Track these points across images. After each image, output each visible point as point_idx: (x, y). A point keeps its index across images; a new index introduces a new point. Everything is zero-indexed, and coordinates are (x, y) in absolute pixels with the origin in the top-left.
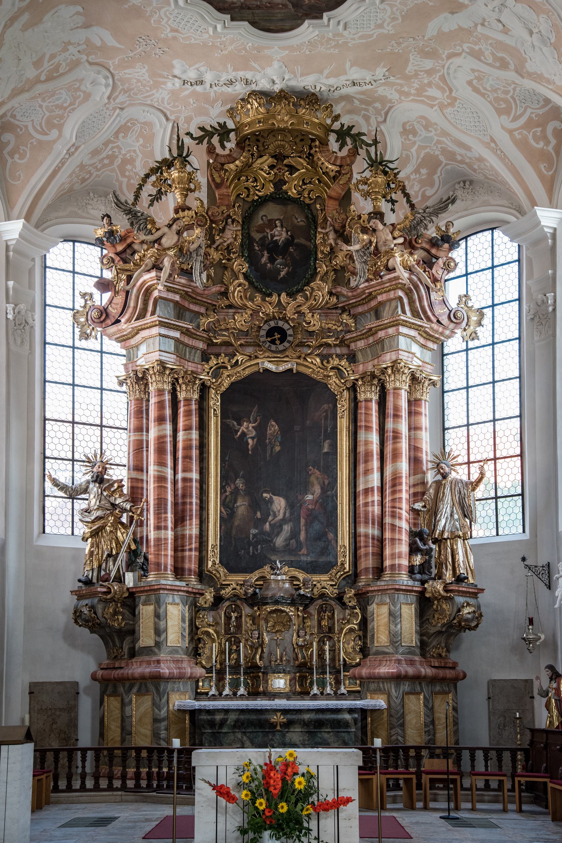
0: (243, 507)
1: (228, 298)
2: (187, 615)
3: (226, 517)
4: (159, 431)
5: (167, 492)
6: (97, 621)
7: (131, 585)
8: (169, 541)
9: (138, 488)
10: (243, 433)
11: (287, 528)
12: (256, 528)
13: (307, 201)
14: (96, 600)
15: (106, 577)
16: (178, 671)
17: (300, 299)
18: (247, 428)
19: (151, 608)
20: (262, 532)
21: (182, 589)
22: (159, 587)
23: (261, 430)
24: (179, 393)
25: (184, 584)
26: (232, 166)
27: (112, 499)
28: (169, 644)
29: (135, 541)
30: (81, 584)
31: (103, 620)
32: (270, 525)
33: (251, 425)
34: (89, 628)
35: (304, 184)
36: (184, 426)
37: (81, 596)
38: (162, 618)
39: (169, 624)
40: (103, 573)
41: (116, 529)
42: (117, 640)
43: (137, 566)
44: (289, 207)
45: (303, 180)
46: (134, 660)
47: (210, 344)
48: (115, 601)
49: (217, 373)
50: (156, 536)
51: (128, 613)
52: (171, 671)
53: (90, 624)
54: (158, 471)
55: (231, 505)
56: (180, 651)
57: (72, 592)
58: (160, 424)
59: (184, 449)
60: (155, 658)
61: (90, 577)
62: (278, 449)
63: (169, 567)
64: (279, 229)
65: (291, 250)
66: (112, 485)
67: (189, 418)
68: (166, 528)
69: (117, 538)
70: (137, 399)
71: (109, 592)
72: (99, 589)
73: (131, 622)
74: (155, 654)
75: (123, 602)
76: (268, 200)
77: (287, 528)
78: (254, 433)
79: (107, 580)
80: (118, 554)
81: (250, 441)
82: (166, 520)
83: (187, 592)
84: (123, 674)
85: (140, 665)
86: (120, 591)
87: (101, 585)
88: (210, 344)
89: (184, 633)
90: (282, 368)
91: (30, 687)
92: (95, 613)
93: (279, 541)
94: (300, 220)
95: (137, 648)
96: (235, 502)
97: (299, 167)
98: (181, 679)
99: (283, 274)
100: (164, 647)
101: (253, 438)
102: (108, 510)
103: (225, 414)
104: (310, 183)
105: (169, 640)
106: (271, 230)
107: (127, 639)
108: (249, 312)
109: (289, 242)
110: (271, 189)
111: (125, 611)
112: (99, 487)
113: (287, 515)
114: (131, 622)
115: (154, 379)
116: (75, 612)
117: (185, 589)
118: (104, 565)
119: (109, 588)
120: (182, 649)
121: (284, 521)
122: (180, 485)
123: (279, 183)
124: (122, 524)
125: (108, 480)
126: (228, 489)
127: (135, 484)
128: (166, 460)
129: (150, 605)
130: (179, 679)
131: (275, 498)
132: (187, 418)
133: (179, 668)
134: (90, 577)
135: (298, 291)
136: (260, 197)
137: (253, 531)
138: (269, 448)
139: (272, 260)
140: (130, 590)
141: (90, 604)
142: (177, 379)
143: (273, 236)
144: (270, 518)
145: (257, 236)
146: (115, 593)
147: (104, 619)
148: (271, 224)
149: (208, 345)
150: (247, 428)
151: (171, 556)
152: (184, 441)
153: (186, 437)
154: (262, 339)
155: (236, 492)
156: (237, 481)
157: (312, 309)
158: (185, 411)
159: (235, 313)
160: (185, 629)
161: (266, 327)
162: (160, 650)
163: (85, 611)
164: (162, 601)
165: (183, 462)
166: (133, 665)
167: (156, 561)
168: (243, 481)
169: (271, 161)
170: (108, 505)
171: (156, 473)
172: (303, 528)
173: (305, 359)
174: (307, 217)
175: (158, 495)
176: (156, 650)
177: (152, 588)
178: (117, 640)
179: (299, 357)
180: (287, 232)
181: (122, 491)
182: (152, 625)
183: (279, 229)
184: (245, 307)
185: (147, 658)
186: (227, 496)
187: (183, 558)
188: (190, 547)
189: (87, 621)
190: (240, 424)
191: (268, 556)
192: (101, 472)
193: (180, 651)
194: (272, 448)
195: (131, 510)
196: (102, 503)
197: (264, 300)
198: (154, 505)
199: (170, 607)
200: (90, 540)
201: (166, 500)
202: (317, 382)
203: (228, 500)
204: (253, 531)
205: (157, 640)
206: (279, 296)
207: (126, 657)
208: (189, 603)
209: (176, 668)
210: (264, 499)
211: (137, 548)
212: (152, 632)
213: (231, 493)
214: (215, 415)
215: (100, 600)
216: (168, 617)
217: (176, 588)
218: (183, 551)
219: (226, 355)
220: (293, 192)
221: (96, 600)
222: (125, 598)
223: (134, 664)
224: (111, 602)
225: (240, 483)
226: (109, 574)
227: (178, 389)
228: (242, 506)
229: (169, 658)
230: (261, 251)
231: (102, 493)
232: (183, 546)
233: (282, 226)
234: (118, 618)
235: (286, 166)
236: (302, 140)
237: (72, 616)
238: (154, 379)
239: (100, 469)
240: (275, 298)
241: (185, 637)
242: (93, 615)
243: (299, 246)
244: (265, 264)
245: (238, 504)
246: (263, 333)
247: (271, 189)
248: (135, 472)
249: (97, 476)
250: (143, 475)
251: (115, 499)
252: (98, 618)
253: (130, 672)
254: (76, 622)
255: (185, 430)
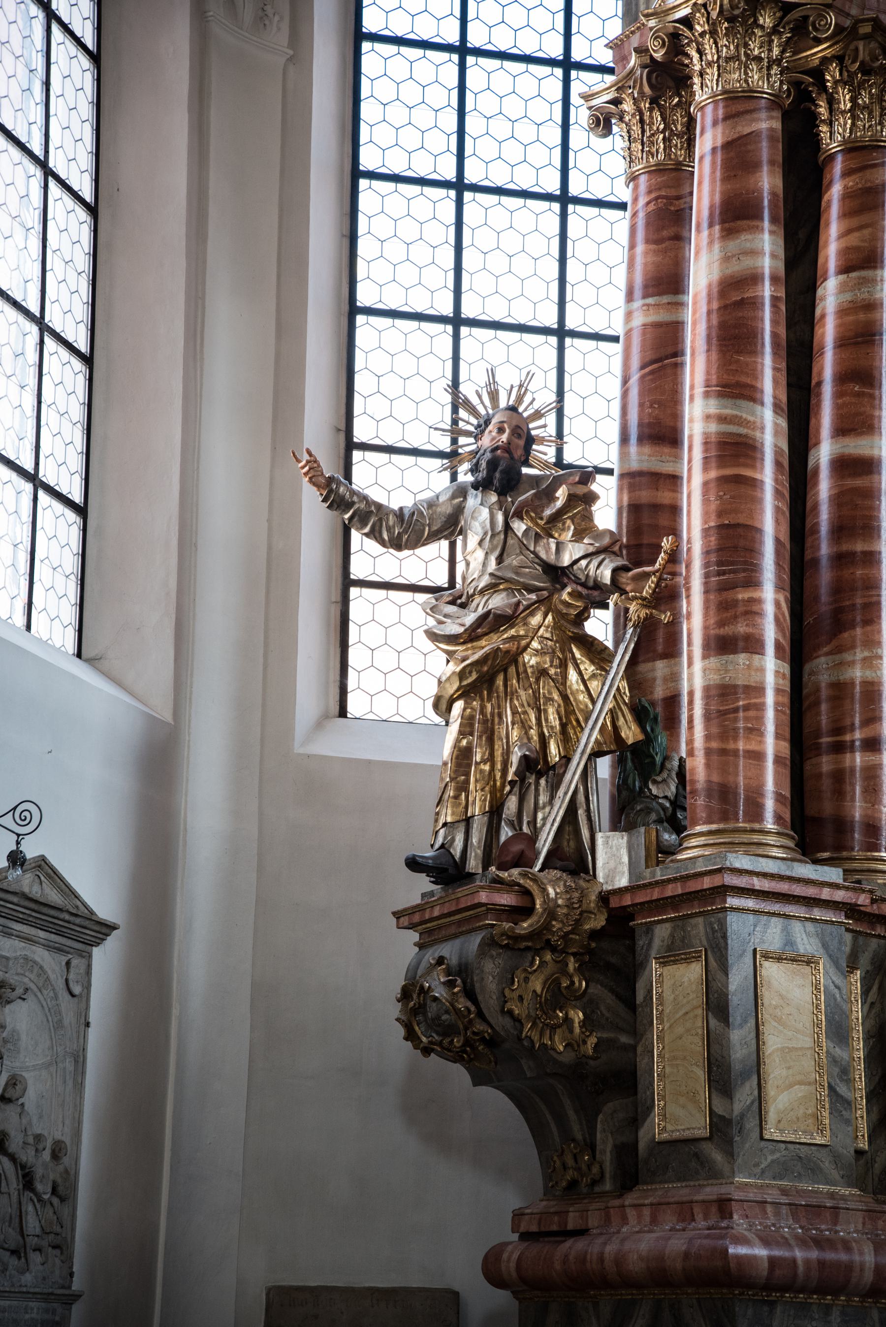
2: (857, 1012)
4: (726, 259)
5: (760, 501)
6: (479, 1026)
7: (623, 881)
8: (770, 698)
9: (656, 507)
14: (475, 941)
15: (516, 848)
16: (814, 1254)
19: (693, 972)
21: (826, 894)
22: (717, 881)
24: (824, 128)
25: (834, 874)
27: (547, 550)
28: (772, 1132)
29: (640, 714)
30: (423, 883)
31: (501, 1023)
34: (457, 1057)
36: (844, 252)
37: (430, 932)
38: (736, 1016)
39: (773, 1042)
40: (506, 833)
41: (563, 665)
42: (571, 1114)
43: (648, 811)
46: (630, 1199)
48: (554, 949)
50: (715, 678)
51: (609, 999)
52: (777, 1253)
53: (457, 1042)
54: (722, 419)
56: (827, 1165)
57: (398, 915)
58: (729, 233)
59: (842, 343)
60: (710, 1192)
61: (457, 849)
63: (770, 804)
66: (549, 495)
67: (865, 218)
68: (754, 645)
69: (565, 698)
70: (658, 170)
71: (527, 911)
72: (483, 897)
73: (624, 1039)
74: (714, 1174)
75: (590, 952)
79: (523, 860)
80: (566, 759)
82: (752, 610)
83: (851, 910)
84: (582, 1259)
85: (654, 1221)
86: (569, 906)
87: (498, 881)
89: (842, 1089)
91: (268, 1294)
92: (470, 994)
95: (642, 1145)
98: (836, 1293)
100: (747, 1145)
102: (530, 589)
105: (772, 1116)
107: (609, 1107)
111: (596, 990)
112: (500, 504)
114: (624, 1039)
115: (710, 54)
116: (406, 994)
117: (840, 896)
118: (512, 804)
119: (526, 893)
120: (837, 1158)
122: (824, 488)
124: (591, 646)
125: (535, 481)
127: (645, 496)
128: (755, 373)
129: (688, 959)
130: (822, 1289)
132: (855, 222)
133: (819, 1243)
134: (457, 849)
140: (614, 903)
141: (454, 961)
142: (818, 74)
146: (551, 913)
147: (507, 1022)
151: (778, 760)
152: (842, 312)
153: (848, 296)
158: (847, 196)
160: (845, 1073)
162: (730, 1154)
163: (438, 988)
164: (733, 943)
165: (838, 395)
166: (625, 1220)
167: (716, 778)
170: (534, 576)
171: (713, 427)
175: (720, 514)
176: (717, 1157)
177: (694, 886)
178: (571, 1114)
181: (588, 517)
182: (696, 1045)
185: (680, 1191)
187: (840, 778)
188: (868, 732)
189: (448, 1031)
192: (507, 448)
193: (827, 1165)
195: (616, 586)
196: (507, 562)
198: (706, 553)
199: (771, 970)
200: (459, 706)
201: (755, 532)
205: (719, 1110)
207: (608, 1186)
208: (865, 960)
209: (803, 1242)
211: (649, 740)
212: (701, 1074)
215: (490, 943)
216: (765, 1015)
217: (798, 890)
218: (840, 748)
221: (475, 941)
222: (594, 934)
223: (631, 1213)
224: (538, 952)
226: (533, 839)
227: (823, 110)
229: (772, 1195)
231: (507, 527)
232: (838, 729)
234: (567, 1020)
237: (395, 1010)
238: (710, 54)
239: (504, 437)
241: (848, 1104)
242: (462, 1004)
248: (647, 449)
249: (493, 464)
250: (678, 458)
251: (559, 546)
252: (480, 1014)
253: (610, 1249)
254: (411, 1035)
255: (844, 269)
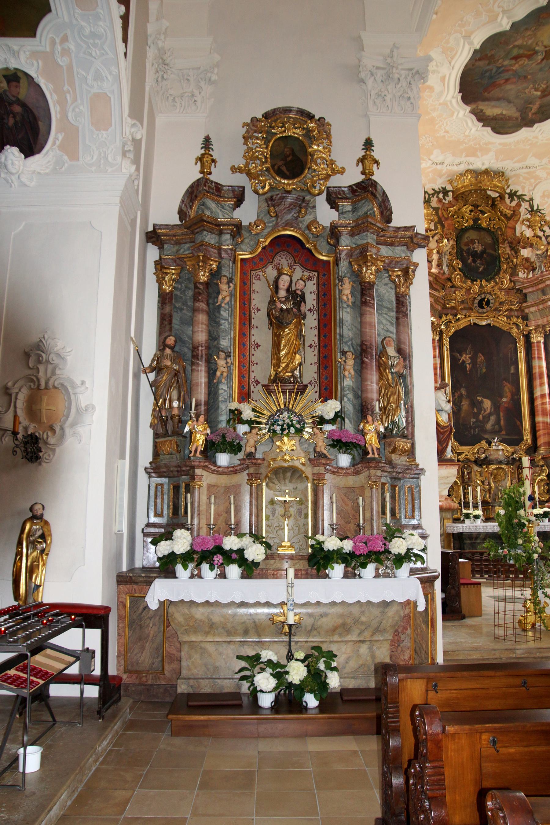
0: (466, 405)
1: (451, 282)
3: (456, 411)
10: (463, 361)
11: (493, 418)
12: (474, 418)
13: (492, 230)
17: (492, 283)
18: (466, 358)
20: (478, 420)
23: (474, 359)
26: (452, 209)
32: (483, 416)
33: (468, 356)
35: (490, 220)
44: (482, 233)
45: (490, 219)
47: (444, 307)
49: (447, 326)
55: (458, 404)
62: (484, 370)
64: (477, 244)
65: (485, 256)
76: (470, 229)
77: (493, 418)
78: (470, 361)
81: (468, 365)
88: (444, 307)
90: (484, 323)
93: (489, 426)
94: (489, 240)
96: (461, 402)
97: (486, 211)
99: (481, 269)
101: (469, 364)
103: (452, 350)
104: (494, 220)
106: (473, 245)
108: (464, 290)
109: (483, 252)
110: (471, 222)
113: (492, 410)
121: (490, 414)
123: (476, 220)
126: (457, 394)
131: (484, 400)
135: (491, 279)
136: (466, 227)
137: (473, 420)
138: (479, 370)
139: (474, 261)
143: (474, 248)
144: (482, 412)
145: (465, 248)
148: (472, 242)
149: (443, 309)
150: (466, 358)
154: (475, 305)
155: (461, 396)
156: (462, 390)
157: (500, 289)
159: (456, 290)
161: (479, 298)
168: (465, 389)
169: (470, 208)
172: (502, 418)
173: (498, 318)
174: (493, 239)
179: (494, 317)
180: (482, 246)
183: (477, 244)
184: (461, 288)
186: (456, 399)
190: (461, 356)
191: (483, 435)
194: (481, 370)
197: (472, 283)
202: (505, 332)
203: (457, 401)
204: (473, 420)
206: (481, 281)
210: (478, 401)
213: (458, 397)
214: (447, 351)
219: (451, 315)
220: (484, 225)
225: (463, 391)
228: (465, 404)
230: (468, 256)
233: (479, 243)
235: (479, 210)
236: (487, 198)
240: (479, 282)
243: (489, 255)
244: (471, 264)
245: (463, 403)
246: (476, 301)
247: (471, 222)
